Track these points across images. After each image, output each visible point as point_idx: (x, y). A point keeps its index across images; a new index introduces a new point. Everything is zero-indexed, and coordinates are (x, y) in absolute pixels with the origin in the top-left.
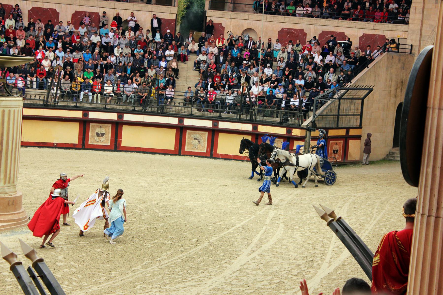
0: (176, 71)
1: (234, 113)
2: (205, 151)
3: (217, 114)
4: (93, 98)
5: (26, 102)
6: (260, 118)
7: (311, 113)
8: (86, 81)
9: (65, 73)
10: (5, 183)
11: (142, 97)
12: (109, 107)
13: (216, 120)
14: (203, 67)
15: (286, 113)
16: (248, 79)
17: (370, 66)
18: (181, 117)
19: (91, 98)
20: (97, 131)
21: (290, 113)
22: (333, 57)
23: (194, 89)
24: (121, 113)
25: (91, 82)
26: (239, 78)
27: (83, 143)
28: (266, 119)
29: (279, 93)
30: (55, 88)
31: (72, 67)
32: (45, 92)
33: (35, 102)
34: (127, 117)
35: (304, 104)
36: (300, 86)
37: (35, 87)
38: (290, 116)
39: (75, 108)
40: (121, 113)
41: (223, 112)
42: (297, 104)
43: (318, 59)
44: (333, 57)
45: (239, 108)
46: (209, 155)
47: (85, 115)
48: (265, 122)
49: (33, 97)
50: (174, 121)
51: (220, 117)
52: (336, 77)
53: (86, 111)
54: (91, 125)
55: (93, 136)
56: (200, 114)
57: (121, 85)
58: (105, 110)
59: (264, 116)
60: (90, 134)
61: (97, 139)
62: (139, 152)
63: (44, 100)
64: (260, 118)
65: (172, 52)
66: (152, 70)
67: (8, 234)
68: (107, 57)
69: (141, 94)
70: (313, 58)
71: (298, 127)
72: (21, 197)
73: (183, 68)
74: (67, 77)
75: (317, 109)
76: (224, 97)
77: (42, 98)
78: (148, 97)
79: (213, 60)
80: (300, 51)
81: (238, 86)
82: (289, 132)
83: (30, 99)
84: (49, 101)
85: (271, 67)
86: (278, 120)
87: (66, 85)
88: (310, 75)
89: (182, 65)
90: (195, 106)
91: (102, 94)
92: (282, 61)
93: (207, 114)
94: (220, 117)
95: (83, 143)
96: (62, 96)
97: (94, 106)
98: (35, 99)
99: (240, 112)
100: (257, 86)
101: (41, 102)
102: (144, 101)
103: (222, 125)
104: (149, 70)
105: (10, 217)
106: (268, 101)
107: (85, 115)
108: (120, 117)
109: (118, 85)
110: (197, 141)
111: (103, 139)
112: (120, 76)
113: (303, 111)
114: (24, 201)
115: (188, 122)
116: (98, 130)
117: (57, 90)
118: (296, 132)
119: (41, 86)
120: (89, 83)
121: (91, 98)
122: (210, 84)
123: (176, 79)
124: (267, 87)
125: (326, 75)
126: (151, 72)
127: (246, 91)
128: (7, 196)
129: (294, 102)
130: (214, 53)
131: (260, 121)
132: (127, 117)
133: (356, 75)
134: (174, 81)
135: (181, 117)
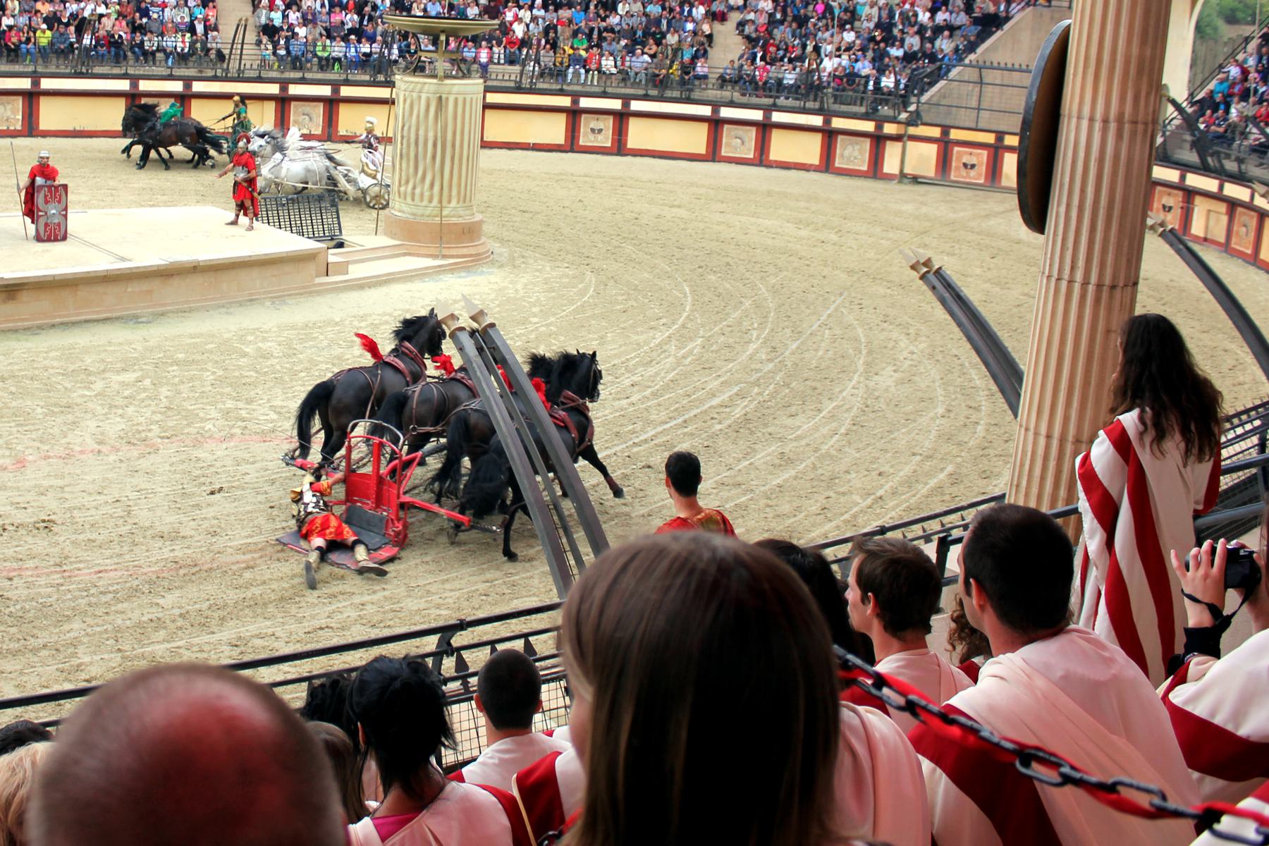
0: (710, 37)
1: (797, 99)
2: (751, 156)
3: (768, 101)
4: (586, 77)
5: (490, 83)
6: (836, 107)
7: (914, 99)
8: (577, 52)
9: (547, 42)
10: (458, 203)
11: (658, 75)
12: (609, 90)
13: (768, 110)
14: (748, 29)
15: (876, 99)
16: (817, 49)
17: (1007, 27)
18: (716, 106)
19: (583, 77)
20: (592, 126)
21: (881, 99)
22: (948, 14)
23: (736, 65)
24: (626, 99)
25: (583, 53)
26: (804, 46)
27: (572, 144)
28: (844, 108)
29: (865, 68)
30: (532, 63)
31: (556, 32)
32: (517, 68)
33: (504, 84)
34: (636, 106)
35: (902, 86)
36: (897, 58)
37: (502, 61)
38: (880, 104)
39: (561, 93)
40: (626, 99)
41: (778, 97)
42: (892, 85)
43: (924, 17)
44: (948, 14)
45: (803, 92)
46: (758, 162)
47: (575, 102)
48: (843, 112)
49: (500, 77)
50: (706, 111)
51: (774, 105)
52: (953, 45)
53: (576, 96)
54: (583, 116)
55: (585, 134)
56: (745, 100)
57: (628, 59)
58: (604, 95)
59: (842, 103)
60: (582, 130)
61: (591, 137)
62: (654, 157)
63: (515, 82)
64: (836, 107)
65: (702, 10)
66: (673, 35)
67: (463, 274)
68: (607, 17)
69: (657, 72)
70: (916, 15)
71: (893, 120)
72: (481, 222)
73: (719, 32)
74: (548, 46)
75: (922, 92)
76: (780, 76)
77: (513, 78)
78: (667, 76)
79: (763, 20)
80: (898, 5)
81: (801, 59)
82: (879, 127)
83: (496, 79)
84: (523, 81)
85: (852, 29)
86: (863, 110)
87: (547, 58)
88: (913, 42)
89: (717, 26)
90: (737, 88)
91: (599, 72)
92: (869, 20)
93: (755, 100)
94: (774, 105)
95: (572, 144)
96: (542, 75)
97: (588, 89)
98: (503, 80)
99: (805, 97)
100: (830, 59)
101: (512, 84)
102: (661, 81)
103: (777, 117)
104: (669, 36)
105: (465, 251)
106: (848, 81)
107: (575, 102)
108: (626, 104)
109: (623, 58)
110: (739, 141)
111: (600, 137)
112: (626, 45)
113: (902, 96)
114: (485, 227)
115: (726, 112)
116: (594, 124)
117: (534, 66)
118: (889, 129)
119: (511, 61)
120: (580, 55)
121: (583, 77)
122: (759, 55)
123: (708, 49)
124: (845, 60)
125: (938, 43)
126: (672, 39)
127: (815, 66)
128: (460, 220)
129: (888, 82)
130: (766, 9)
131: (835, 111)
132: (636, 106)
133: (983, 41)
134: (706, 52)
135: (716, 106)
